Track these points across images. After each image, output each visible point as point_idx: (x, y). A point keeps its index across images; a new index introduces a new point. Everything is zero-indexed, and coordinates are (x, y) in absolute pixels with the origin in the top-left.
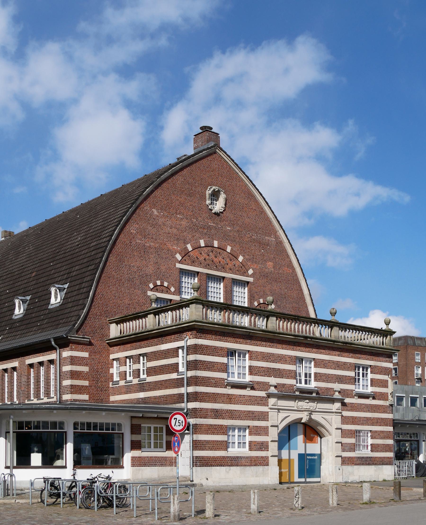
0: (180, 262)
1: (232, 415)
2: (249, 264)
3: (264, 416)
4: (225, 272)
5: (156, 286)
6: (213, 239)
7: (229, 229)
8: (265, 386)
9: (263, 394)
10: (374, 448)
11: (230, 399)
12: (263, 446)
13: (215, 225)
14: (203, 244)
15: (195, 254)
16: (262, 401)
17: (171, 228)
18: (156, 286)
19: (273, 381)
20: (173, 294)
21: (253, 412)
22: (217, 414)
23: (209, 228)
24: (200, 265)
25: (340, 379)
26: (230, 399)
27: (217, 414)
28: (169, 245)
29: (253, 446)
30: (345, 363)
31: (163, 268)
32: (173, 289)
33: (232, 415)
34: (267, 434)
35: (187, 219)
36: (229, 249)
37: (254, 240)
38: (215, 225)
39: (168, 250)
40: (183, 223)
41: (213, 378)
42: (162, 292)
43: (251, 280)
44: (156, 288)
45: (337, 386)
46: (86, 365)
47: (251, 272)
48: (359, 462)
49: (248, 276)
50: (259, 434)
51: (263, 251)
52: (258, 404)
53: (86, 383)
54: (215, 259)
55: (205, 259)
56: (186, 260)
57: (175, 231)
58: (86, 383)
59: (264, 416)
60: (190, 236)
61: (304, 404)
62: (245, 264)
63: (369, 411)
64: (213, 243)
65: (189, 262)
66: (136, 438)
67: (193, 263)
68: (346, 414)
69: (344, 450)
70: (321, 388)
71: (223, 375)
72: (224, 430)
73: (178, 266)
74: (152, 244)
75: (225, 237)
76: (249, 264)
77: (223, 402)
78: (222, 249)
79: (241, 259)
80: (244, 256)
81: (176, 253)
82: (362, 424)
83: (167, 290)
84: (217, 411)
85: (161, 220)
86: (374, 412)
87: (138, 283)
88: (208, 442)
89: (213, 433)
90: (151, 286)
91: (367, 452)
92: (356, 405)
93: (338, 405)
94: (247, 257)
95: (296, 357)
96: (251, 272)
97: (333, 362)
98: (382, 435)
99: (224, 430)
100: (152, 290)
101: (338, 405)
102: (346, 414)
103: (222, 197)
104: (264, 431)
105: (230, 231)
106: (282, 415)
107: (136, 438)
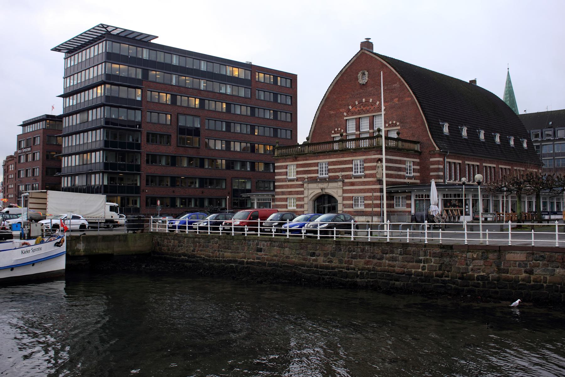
3: (302, 193)
5: (335, 131)
9: (301, 183)
10: (366, 206)
12: (302, 206)
14: (357, 103)
18: (335, 131)
19: (305, 176)
22: (283, 193)
27: (283, 193)
29: (298, 206)
48: (355, 214)
54: (364, 109)
59: (302, 193)
61: (321, 185)
63: (362, 185)
68: (345, 188)
71: (285, 177)
72: (286, 200)
82: (358, 193)
88: (279, 205)
90: (333, 132)
91: (361, 208)
93: (340, 184)
99: (286, 200)
101: (340, 184)
102: (345, 188)
103: (366, 73)
104: (302, 199)
106: (310, 191)
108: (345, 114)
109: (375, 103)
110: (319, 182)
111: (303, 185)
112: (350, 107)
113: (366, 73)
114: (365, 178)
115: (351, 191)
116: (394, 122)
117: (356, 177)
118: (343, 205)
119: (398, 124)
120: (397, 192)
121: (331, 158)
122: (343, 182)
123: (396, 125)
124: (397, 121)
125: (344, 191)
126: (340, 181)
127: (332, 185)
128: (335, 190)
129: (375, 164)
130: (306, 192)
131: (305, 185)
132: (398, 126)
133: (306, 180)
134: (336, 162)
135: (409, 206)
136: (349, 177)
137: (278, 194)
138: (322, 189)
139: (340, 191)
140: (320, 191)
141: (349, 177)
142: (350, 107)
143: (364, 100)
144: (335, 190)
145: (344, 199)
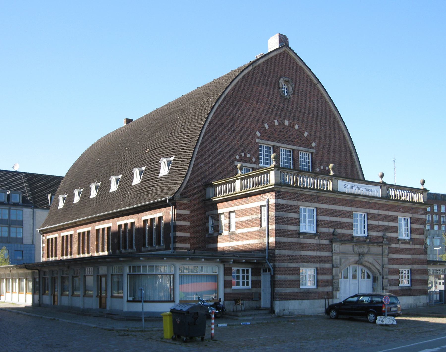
0: (259, 138)
14: (276, 122)
20: (254, 163)
30: (391, 216)
32: (254, 160)
36: (297, 127)
43: (314, 151)
46: (188, 220)
49: (313, 148)
53: (187, 235)
57: (255, 113)
58: (187, 235)
63: (409, 254)
64: (285, 122)
66: (228, 278)
70: (373, 237)
73: (258, 141)
80: (308, 132)
81: (256, 131)
84: (291, 256)
92: (399, 249)
94: (311, 133)
96: (314, 144)
97: (382, 215)
107: (228, 278)
108: (258, 134)
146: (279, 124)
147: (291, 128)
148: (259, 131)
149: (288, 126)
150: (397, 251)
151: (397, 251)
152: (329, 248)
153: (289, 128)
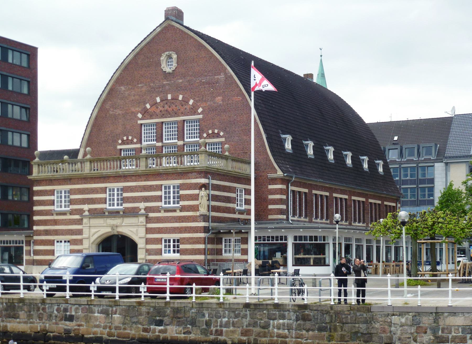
0: (141, 119)
1: (56, 232)
2: (198, 104)
3: (80, 232)
4: (178, 116)
5: (123, 141)
6: (167, 94)
7: (181, 81)
8: (80, 212)
11: (55, 222)
13: (168, 82)
14: (158, 100)
15: (154, 108)
16: (79, 222)
17: (134, 96)
18: (123, 141)
19: (86, 207)
20: (135, 143)
21: (71, 230)
22: (47, 233)
23: (164, 86)
24: (157, 116)
25: (146, 199)
26: (55, 222)
27: (47, 233)
28: (133, 109)
30: (151, 186)
31: (128, 127)
32: (135, 140)
33: (56, 232)
34: (82, 244)
35: (146, 85)
37: (203, 82)
38: (168, 82)
39: (132, 112)
40: (143, 89)
41: (44, 210)
42: (128, 144)
44: (124, 143)
45: (142, 205)
47: (200, 110)
50: (76, 244)
51: (212, 89)
52: (76, 224)
54: (170, 109)
55: (161, 111)
56: (146, 116)
60: (148, 97)
61: (111, 221)
62: (195, 105)
63: (176, 222)
65: (149, 117)
67: (151, 117)
68: (150, 226)
69: (150, 254)
70: (128, 208)
72: (51, 243)
74: (120, 112)
75: (178, 89)
76: (198, 104)
77: (51, 225)
78: (175, 99)
79: (191, 102)
80: (194, 99)
81: (138, 113)
83: (132, 142)
85: (127, 93)
86: (183, 222)
87: (111, 141)
88: (41, 251)
89: (44, 245)
90: (120, 141)
92: (162, 218)
93: (142, 219)
94: (197, 99)
95: (101, 188)
96: (200, 110)
97: (140, 186)
98: (191, 241)
100: (120, 144)
102: (150, 226)
105: (182, 83)
106: (93, 230)
108: (140, 116)
109: (187, 102)
110: (107, 217)
111: (82, 219)
112: (148, 106)
113: (175, 56)
114: (181, 211)
115: (160, 231)
116: (216, 131)
117: (167, 210)
118: (147, 250)
119: (222, 134)
120: (229, 233)
121: (128, 181)
122: (147, 217)
123: (218, 136)
124: (220, 129)
125: (148, 231)
126: (142, 215)
127: (128, 221)
128: (134, 229)
129: (196, 192)
130: (86, 231)
131: (85, 221)
132: (222, 137)
133: (87, 213)
134: (136, 186)
135: (245, 252)
136: (157, 210)
137: (39, 233)
138: (113, 227)
139: (142, 231)
140: (109, 230)
141: (157, 210)
142: (148, 106)
143: (169, 97)
144: (134, 229)
145: (148, 241)
146: (162, 101)
147: (175, 101)
148: (141, 113)
149: (172, 99)
150: (159, 220)
151: (159, 220)
152: (79, 222)
153: (173, 101)
